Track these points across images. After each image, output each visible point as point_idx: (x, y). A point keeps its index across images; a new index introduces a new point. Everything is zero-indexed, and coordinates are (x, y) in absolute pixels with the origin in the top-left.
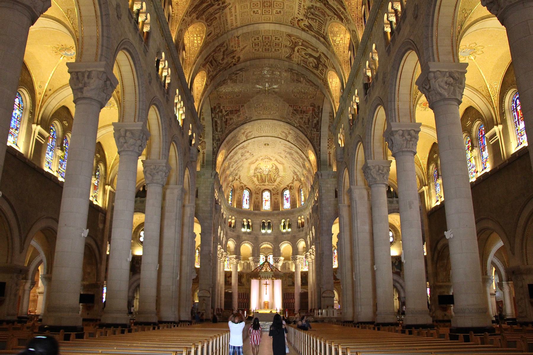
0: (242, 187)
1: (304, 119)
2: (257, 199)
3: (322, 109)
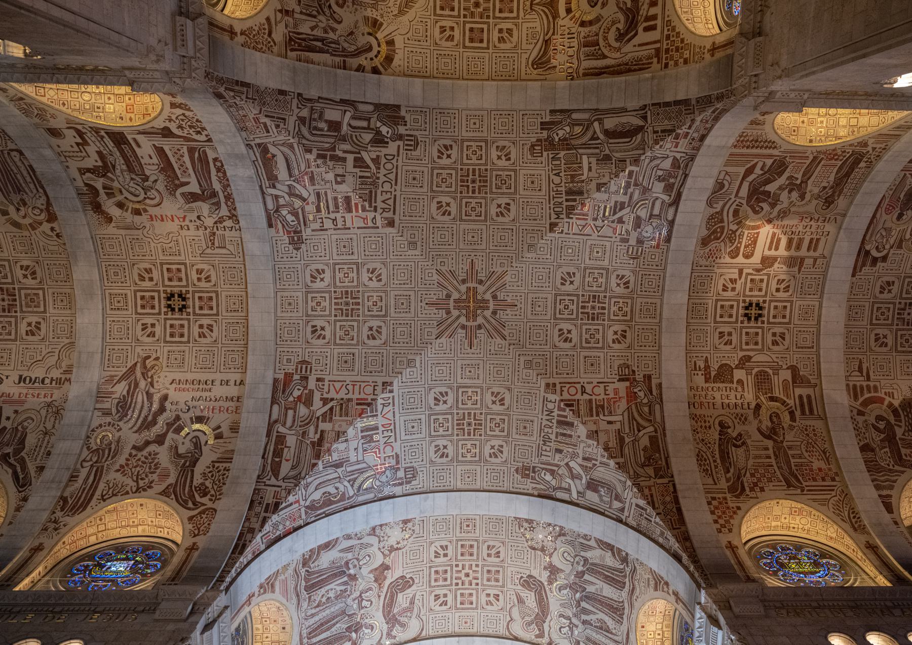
1: (603, 437)
3: (660, 386)
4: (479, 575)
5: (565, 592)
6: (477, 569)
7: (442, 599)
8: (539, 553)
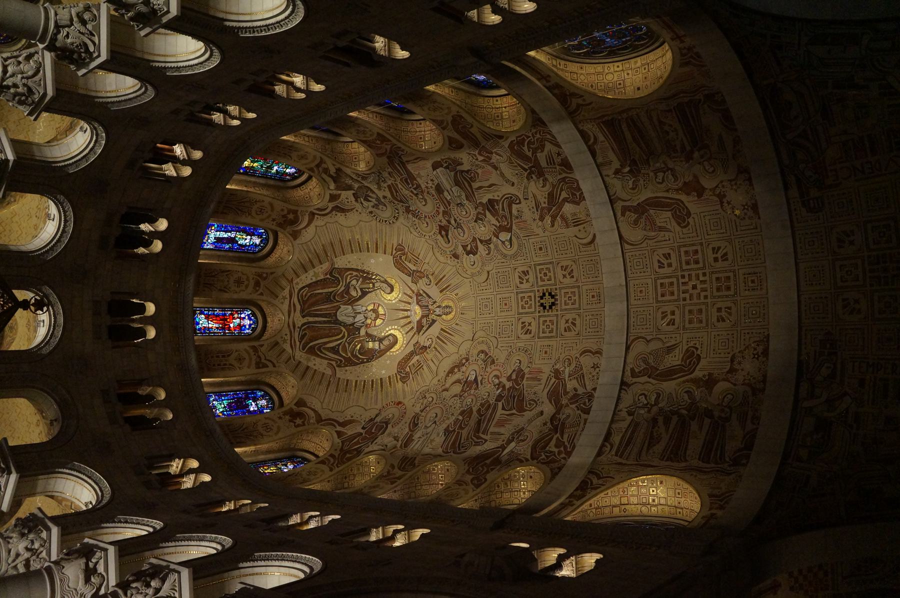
0: (294, 222)
2: (239, 282)
4: (695, 301)
5: (686, 397)
6: (702, 298)
7: (665, 262)
8: (728, 367)
